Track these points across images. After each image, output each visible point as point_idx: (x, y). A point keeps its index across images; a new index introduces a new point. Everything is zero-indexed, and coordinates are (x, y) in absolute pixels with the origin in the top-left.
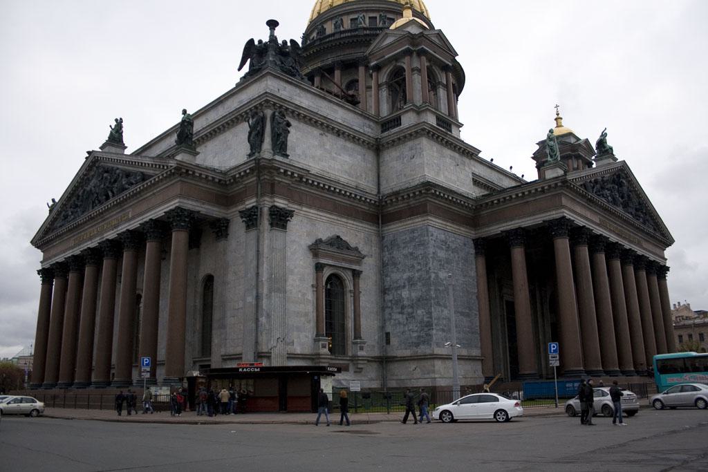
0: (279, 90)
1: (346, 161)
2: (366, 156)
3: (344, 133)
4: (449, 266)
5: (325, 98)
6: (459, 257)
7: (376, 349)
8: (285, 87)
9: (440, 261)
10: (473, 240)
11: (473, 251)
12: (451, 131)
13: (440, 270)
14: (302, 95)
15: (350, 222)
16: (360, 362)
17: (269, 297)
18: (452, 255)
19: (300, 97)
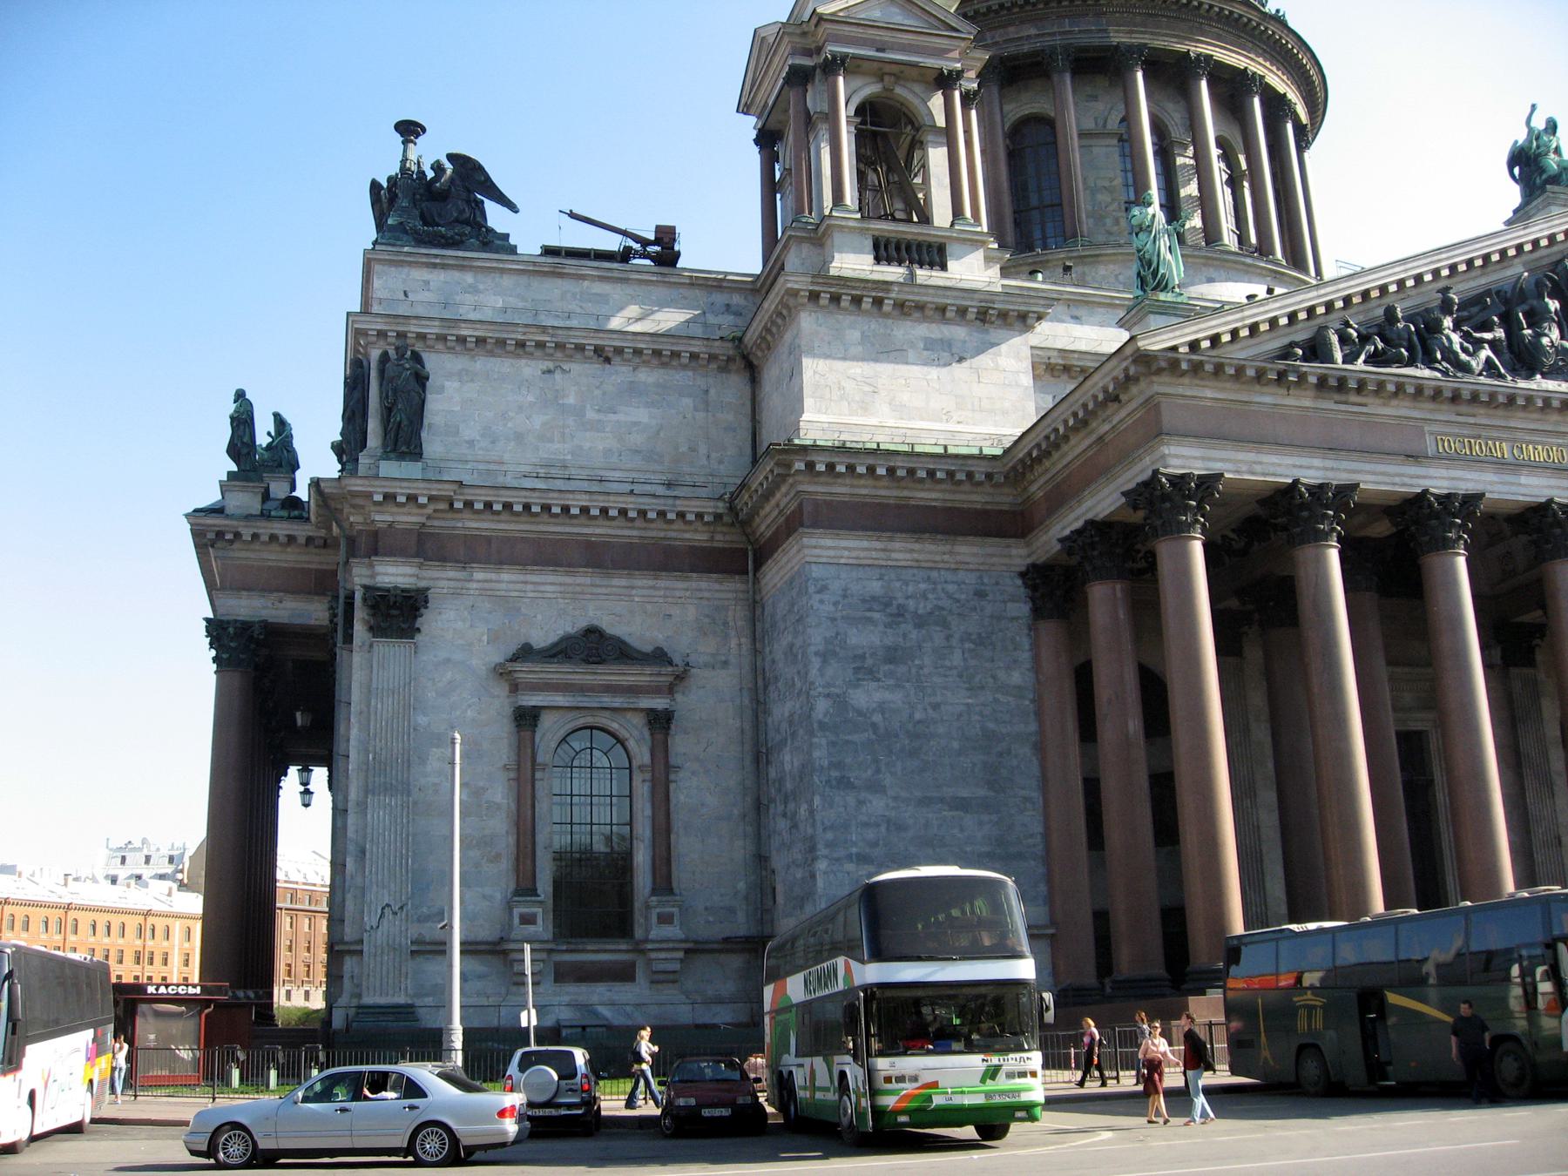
0: (406, 294)
1: (636, 424)
2: (712, 392)
3: (619, 351)
4: (901, 669)
5: (561, 275)
6: (948, 638)
7: (741, 916)
8: (427, 283)
9: (863, 657)
10: (1022, 575)
11: (1023, 609)
12: (944, 267)
13: (855, 684)
14: (481, 287)
15: (639, 583)
16: (653, 955)
17: (362, 807)
18: (914, 635)
19: (474, 290)
